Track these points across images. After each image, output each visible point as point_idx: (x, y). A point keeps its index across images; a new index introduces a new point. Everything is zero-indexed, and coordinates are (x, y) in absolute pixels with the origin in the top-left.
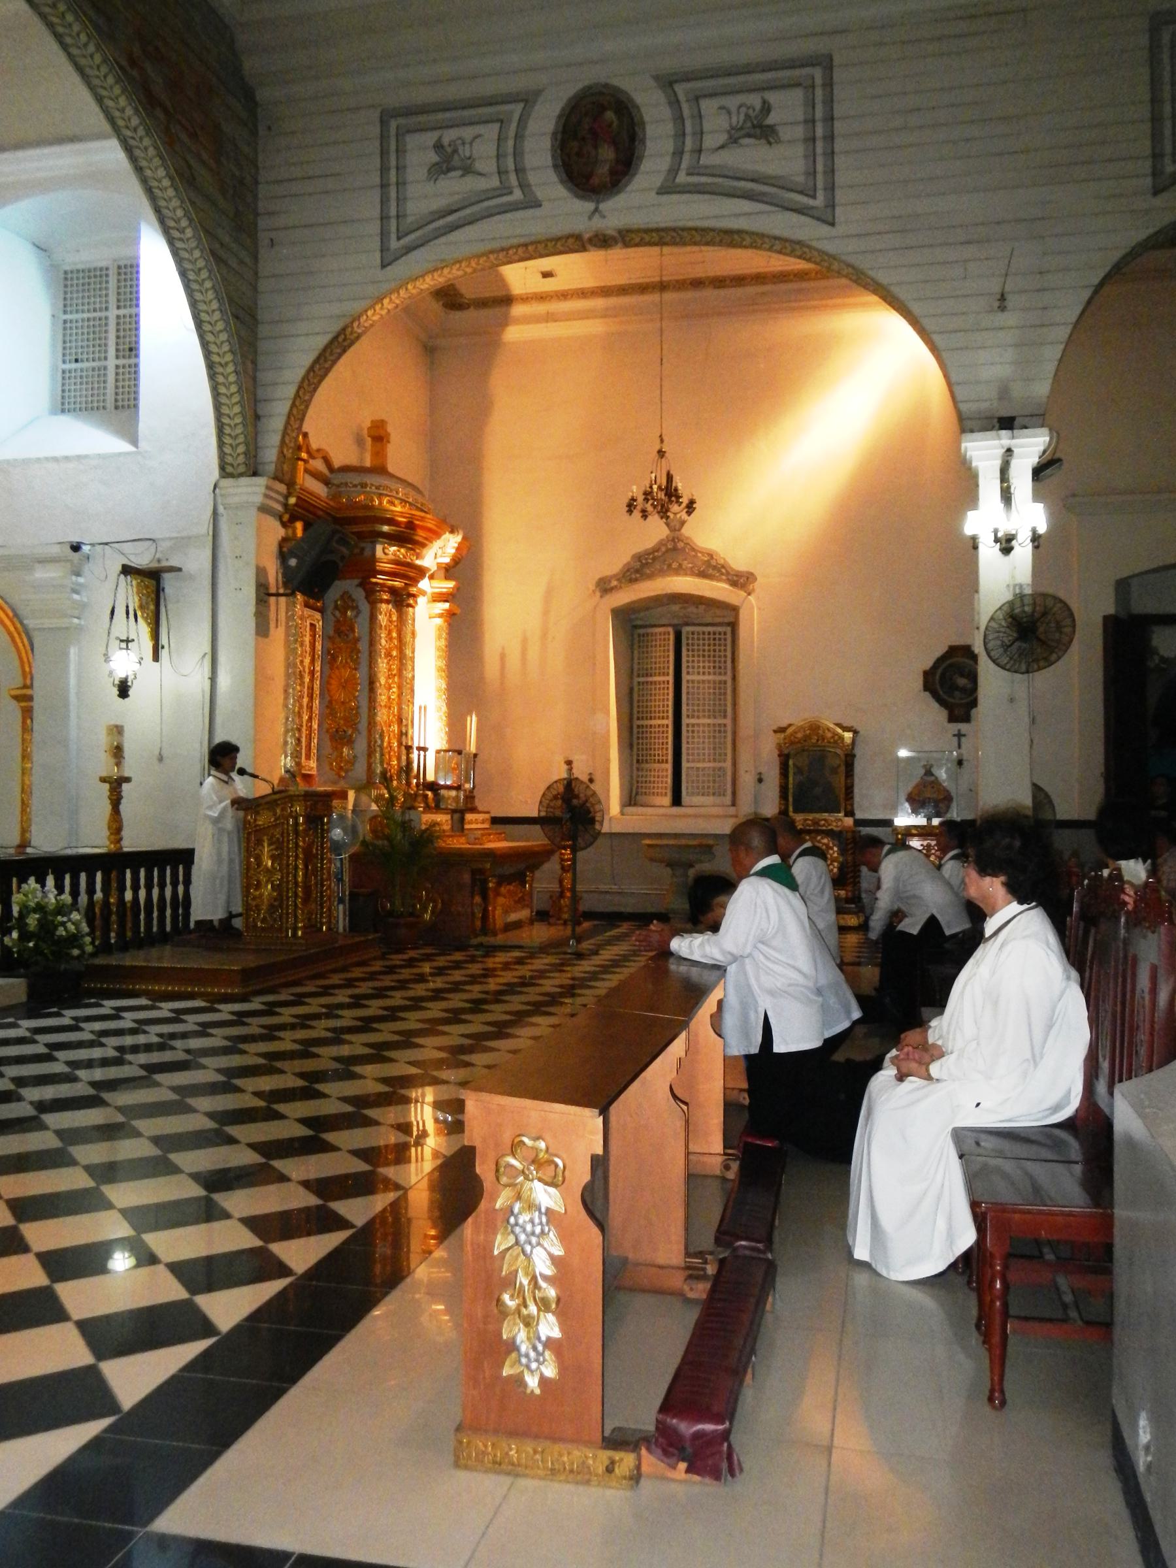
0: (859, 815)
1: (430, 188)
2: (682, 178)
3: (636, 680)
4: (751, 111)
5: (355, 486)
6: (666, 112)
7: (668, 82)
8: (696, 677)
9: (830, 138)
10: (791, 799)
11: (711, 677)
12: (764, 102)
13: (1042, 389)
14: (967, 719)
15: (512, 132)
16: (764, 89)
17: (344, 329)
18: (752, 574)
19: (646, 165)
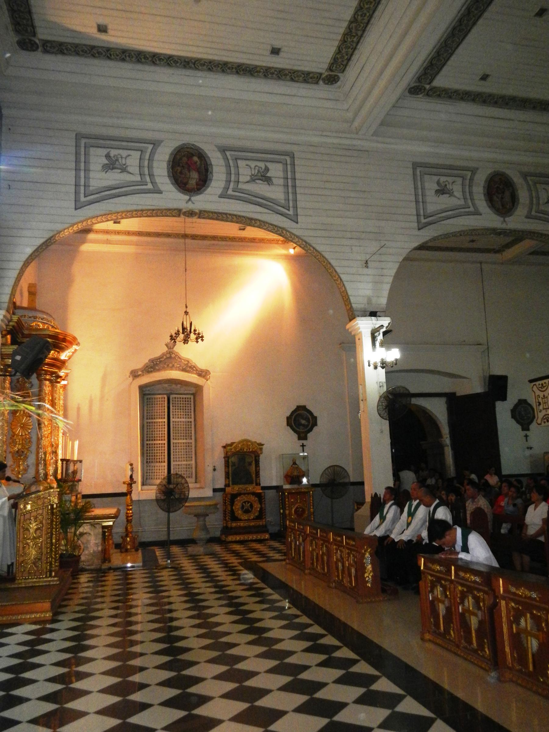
0: (262, 484)
1: (103, 175)
2: (230, 192)
3: (146, 421)
4: (260, 169)
5: (30, 317)
6: (222, 162)
7: (223, 150)
8: (177, 420)
9: (294, 186)
10: (230, 478)
11: (184, 420)
12: (266, 166)
13: (383, 301)
14: (305, 438)
15: (147, 157)
16: (267, 161)
17: (52, 237)
18: (208, 371)
19: (213, 184)
